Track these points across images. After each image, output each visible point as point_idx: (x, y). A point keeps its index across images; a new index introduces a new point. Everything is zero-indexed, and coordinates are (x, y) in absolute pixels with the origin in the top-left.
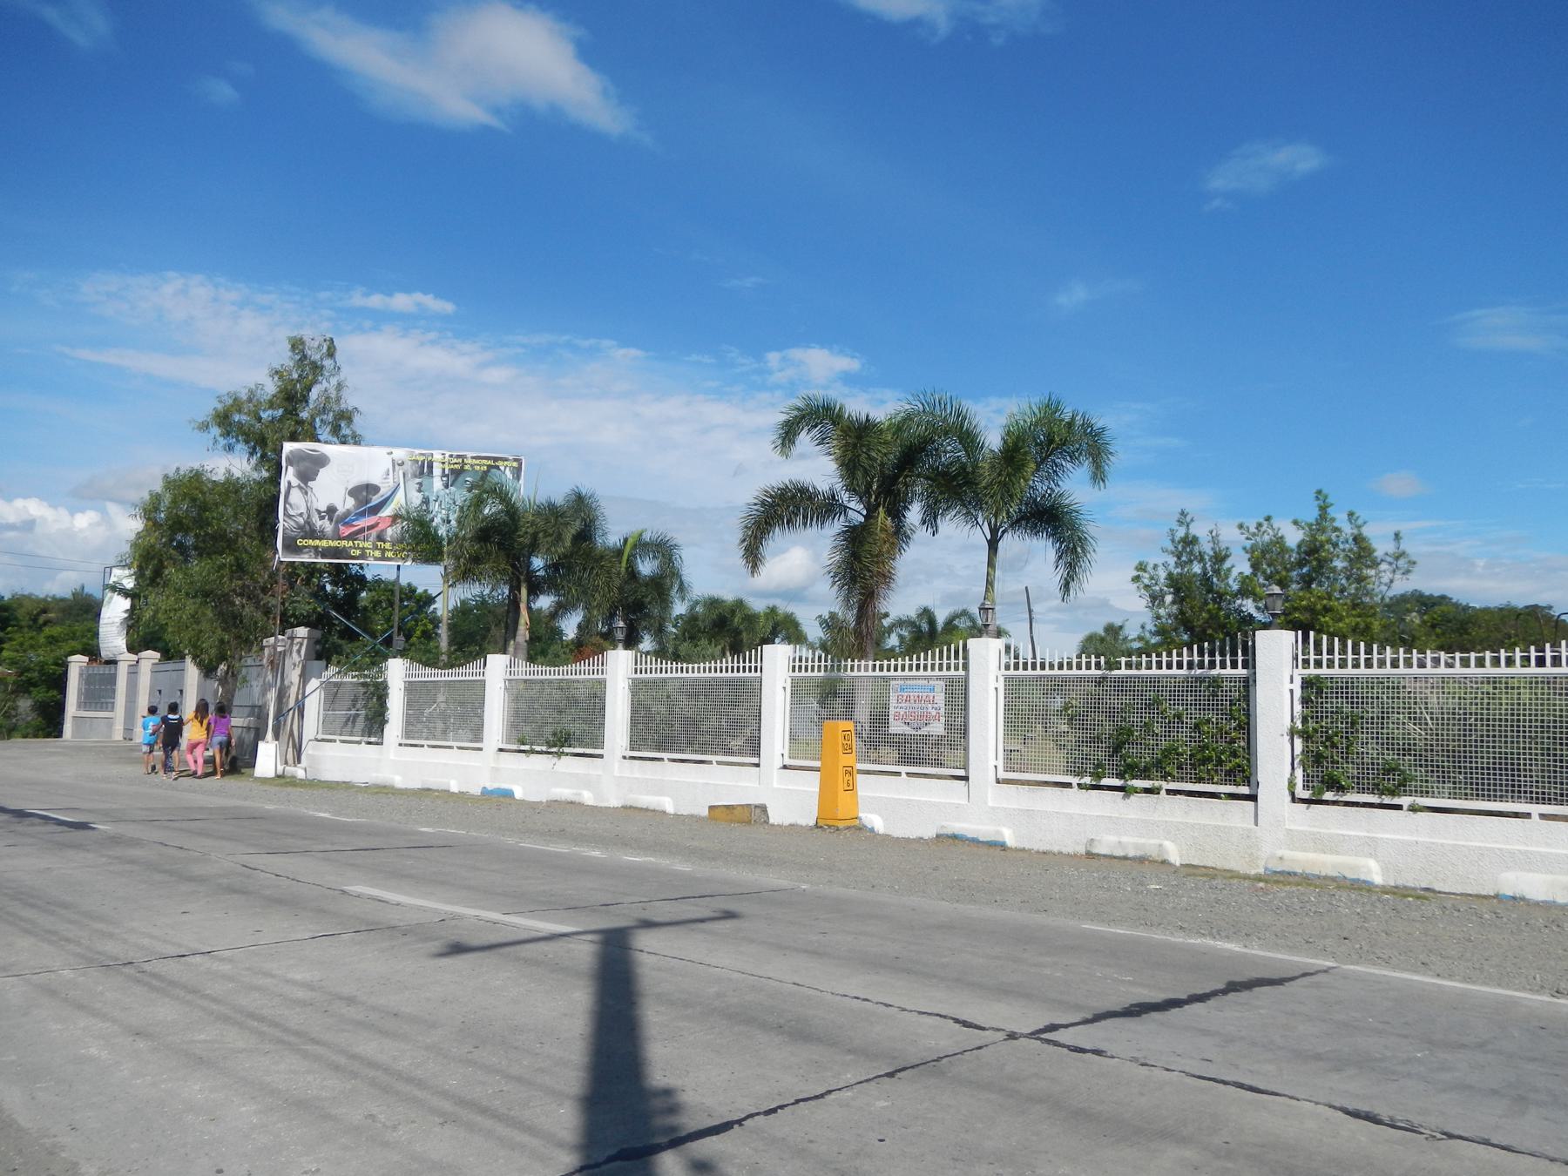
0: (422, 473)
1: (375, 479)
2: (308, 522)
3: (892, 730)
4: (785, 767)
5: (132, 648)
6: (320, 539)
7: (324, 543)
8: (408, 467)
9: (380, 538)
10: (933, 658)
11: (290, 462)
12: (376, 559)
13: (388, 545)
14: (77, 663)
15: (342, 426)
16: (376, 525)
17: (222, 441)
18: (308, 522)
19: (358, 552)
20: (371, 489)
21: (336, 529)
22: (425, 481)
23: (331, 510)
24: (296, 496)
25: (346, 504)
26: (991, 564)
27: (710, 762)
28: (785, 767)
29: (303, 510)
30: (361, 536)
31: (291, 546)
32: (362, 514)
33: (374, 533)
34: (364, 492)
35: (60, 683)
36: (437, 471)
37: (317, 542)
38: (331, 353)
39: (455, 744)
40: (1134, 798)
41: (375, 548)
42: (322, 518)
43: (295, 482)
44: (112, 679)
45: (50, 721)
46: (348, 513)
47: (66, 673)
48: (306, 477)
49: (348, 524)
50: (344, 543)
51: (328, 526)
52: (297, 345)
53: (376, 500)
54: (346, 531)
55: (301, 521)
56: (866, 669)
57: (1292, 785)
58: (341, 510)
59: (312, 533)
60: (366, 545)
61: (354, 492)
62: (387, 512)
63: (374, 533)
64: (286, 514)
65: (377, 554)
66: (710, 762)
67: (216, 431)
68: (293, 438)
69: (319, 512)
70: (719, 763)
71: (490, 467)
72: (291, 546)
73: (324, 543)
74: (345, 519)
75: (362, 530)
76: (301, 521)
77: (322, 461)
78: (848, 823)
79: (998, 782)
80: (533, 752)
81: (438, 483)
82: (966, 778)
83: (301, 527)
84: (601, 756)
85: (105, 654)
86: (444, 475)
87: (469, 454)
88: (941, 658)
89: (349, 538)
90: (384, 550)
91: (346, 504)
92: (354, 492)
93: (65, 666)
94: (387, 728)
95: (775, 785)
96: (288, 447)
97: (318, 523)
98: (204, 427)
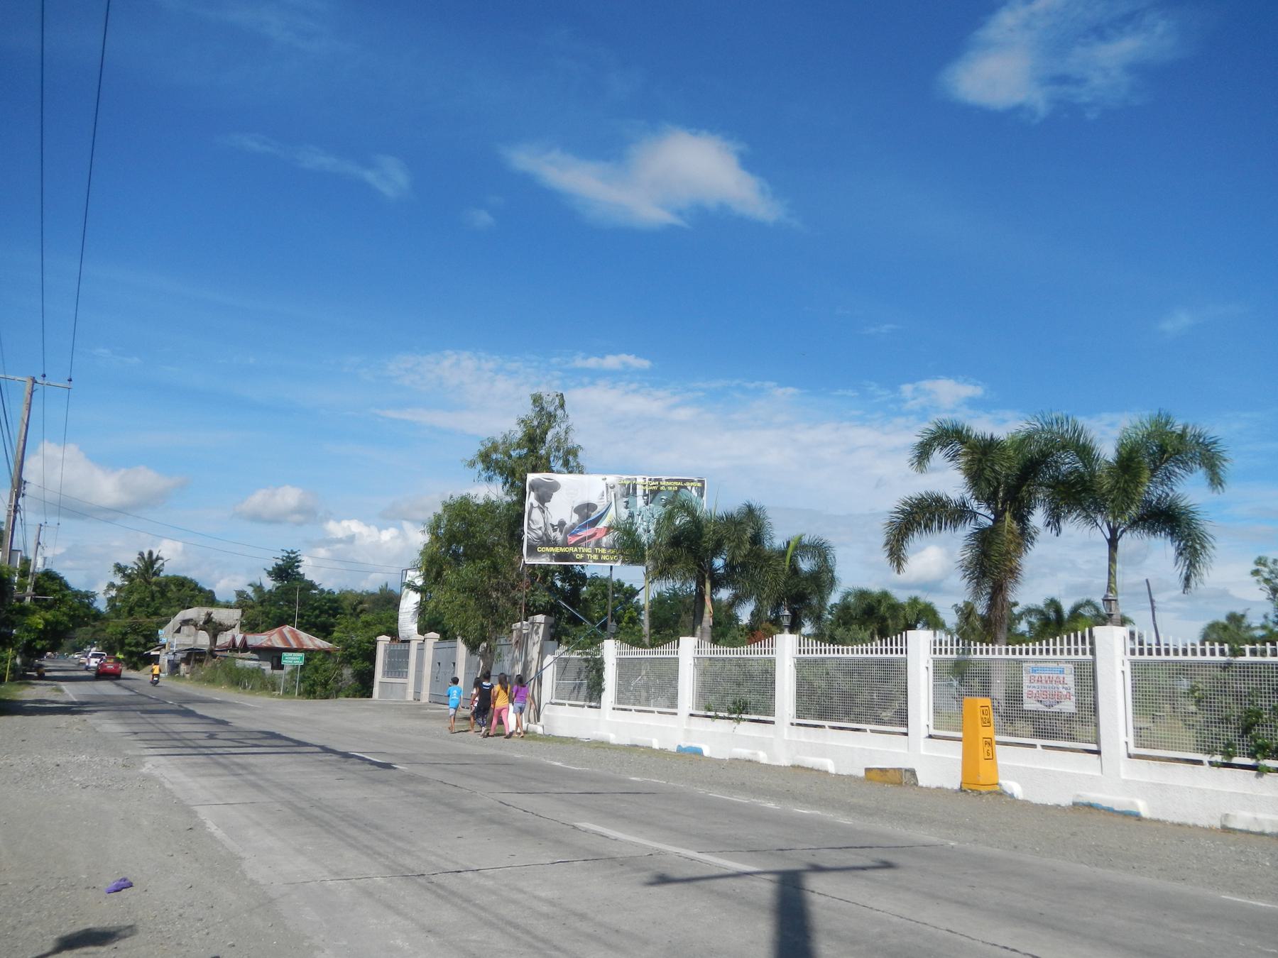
0: (628, 494)
1: (594, 500)
2: (545, 534)
3: (1027, 706)
4: (930, 737)
5: (422, 631)
7: (557, 550)
8: (618, 489)
9: (598, 544)
10: (1062, 644)
11: (532, 488)
12: (595, 561)
13: (603, 551)
14: (383, 641)
15: (570, 461)
16: (594, 535)
17: (484, 475)
18: (545, 534)
20: (590, 507)
21: (565, 538)
22: (631, 499)
23: (562, 524)
24: (536, 514)
25: (572, 519)
26: (1112, 559)
27: (865, 730)
28: (930, 737)
29: (542, 525)
31: (532, 550)
32: (584, 527)
33: (593, 541)
34: (585, 510)
35: (371, 656)
36: (640, 492)
38: (562, 406)
39: (656, 709)
40: (1268, 777)
41: (594, 552)
42: (555, 530)
43: (536, 503)
44: (406, 654)
45: (364, 686)
46: (573, 527)
47: (375, 649)
48: (543, 499)
49: (573, 535)
50: (571, 549)
51: (559, 536)
52: (537, 400)
53: (594, 515)
54: (572, 540)
55: (540, 533)
56: (1000, 653)
58: (569, 523)
61: (578, 510)
62: (603, 524)
63: (593, 541)
65: (595, 557)
66: (865, 730)
67: (480, 466)
68: (534, 470)
70: (872, 731)
71: (679, 487)
73: (557, 550)
74: (572, 531)
75: (584, 539)
76: (540, 533)
77: (554, 487)
79: (1130, 756)
80: (717, 717)
81: (640, 502)
82: (1098, 752)
83: (540, 538)
84: (773, 723)
85: (402, 636)
86: (645, 495)
87: (664, 478)
88: (1069, 644)
89: (573, 545)
90: (600, 555)
91: (572, 519)
92: (578, 510)
93: (375, 643)
94: (604, 695)
95: (923, 752)
96: (531, 477)
98: (472, 464)
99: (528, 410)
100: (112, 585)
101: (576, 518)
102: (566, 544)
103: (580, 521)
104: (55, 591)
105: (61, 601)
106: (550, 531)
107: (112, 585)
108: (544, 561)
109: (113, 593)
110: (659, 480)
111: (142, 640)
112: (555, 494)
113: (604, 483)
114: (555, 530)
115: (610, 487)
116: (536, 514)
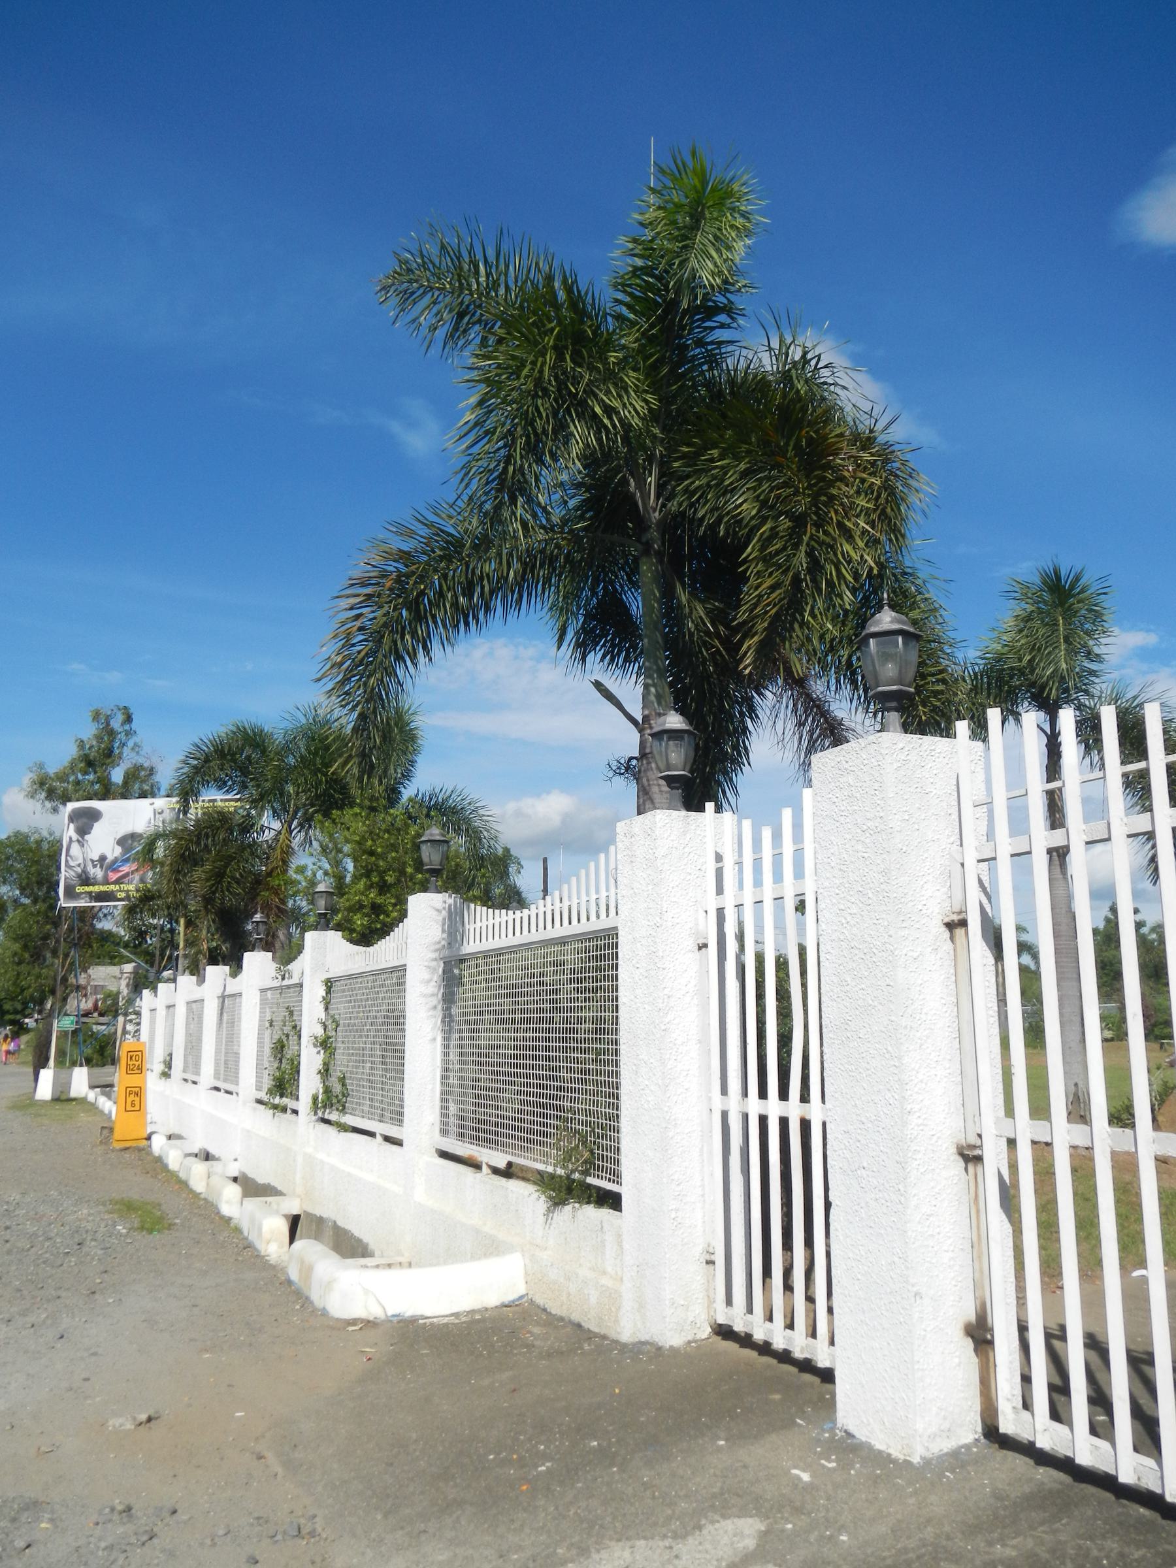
2: (84, 871)
6: (93, 885)
8: (168, 815)
17: (48, 805)
18: (84, 871)
19: (123, 895)
20: (133, 836)
21: (106, 877)
23: (103, 859)
24: (75, 848)
28: (217, 1089)
29: (81, 861)
30: (126, 880)
31: (70, 893)
32: (127, 860)
33: (137, 877)
37: (91, 888)
42: (95, 866)
43: (75, 837)
46: (116, 860)
48: (83, 831)
49: (115, 870)
50: (112, 887)
51: (97, 873)
52: (96, 716)
54: (113, 877)
57: (315, 1099)
58: (110, 858)
59: (85, 880)
61: (121, 842)
64: (67, 865)
69: (93, 861)
72: (70, 893)
74: (113, 866)
75: (127, 875)
76: (79, 870)
77: (95, 816)
78: (128, 1144)
83: (79, 876)
92: (121, 842)
99: (88, 731)
101: (118, 850)
102: (106, 882)
103: (123, 854)
108: (82, 903)
110: (214, 801)
112: (97, 826)
113: (151, 809)
114: (95, 866)
116: (75, 848)
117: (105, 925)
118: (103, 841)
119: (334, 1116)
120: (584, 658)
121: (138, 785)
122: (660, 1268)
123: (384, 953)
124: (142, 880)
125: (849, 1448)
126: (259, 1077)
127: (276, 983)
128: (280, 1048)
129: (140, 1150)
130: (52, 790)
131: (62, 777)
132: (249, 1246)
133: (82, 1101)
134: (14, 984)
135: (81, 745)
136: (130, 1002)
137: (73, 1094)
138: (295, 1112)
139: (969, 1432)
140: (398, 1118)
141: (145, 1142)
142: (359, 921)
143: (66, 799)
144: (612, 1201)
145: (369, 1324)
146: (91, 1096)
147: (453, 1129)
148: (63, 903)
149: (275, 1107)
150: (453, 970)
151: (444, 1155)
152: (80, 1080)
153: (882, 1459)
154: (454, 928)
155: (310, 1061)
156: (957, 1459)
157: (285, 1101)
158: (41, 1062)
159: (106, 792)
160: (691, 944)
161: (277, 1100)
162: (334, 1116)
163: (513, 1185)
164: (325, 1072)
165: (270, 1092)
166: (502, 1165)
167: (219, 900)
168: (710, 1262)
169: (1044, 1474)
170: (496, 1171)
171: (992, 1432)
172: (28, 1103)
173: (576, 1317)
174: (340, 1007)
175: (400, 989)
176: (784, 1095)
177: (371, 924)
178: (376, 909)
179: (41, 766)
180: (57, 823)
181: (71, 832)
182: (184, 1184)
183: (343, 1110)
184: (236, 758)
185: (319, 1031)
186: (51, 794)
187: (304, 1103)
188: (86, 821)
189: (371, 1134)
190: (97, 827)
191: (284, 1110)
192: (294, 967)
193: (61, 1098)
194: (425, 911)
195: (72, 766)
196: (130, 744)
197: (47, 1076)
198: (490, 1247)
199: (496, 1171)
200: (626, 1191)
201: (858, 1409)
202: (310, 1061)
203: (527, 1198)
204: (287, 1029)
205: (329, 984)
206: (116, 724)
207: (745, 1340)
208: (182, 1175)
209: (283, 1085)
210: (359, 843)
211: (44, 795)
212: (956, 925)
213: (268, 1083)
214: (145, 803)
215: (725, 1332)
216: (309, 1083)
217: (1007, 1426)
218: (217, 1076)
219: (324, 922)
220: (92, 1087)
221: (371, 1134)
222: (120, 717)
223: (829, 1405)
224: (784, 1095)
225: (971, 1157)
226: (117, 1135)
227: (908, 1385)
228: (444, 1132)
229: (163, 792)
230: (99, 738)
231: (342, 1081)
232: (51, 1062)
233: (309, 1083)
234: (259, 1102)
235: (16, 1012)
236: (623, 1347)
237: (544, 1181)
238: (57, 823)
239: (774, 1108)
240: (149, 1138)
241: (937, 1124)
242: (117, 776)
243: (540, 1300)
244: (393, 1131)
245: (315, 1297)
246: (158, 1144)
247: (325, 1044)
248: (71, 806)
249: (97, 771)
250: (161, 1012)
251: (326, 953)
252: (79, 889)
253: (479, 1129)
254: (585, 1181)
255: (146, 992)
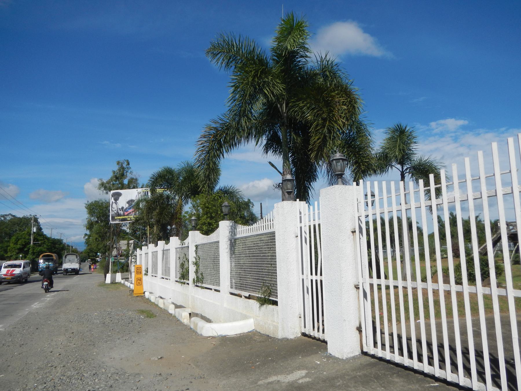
1: (134, 198)
2: (117, 212)
8: (142, 194)
17: (105, 192)
18: (117, 212)
20: (132, 201)
21: (124, 213)
23: (123, 208)
24: (114, 205)
25: (126, 206)
28: (163, 278)
32: (130, 208)
34: (130, 202)
37: (120, 217)
38: (129, 164)
43: (114, 201)
46: (126, 208)
48: (116, 200)
51: (121, 212)
52: (118, 163)
54: (126, 213)
57: (194, 280)
58: (125, 208)
59: (119, 215)
60: (132, 217)
61: (128, 202)
64: (112, 210)
74: (126, 210)
76: (116, 212)
77: (119, 195)
83: (116, 214)
89: (127, 215)
91: (126, 206)
92: (128, 202)
97: (120, 212)
99: (116, 168)
100: (86, 235)
101: (127, 205)
102: (124, 215)
104: (41, 240)
105: (44, 243)
106: (119, 211)
107: (86, 235)
108: (117, 222)
109: (87, 237)
111: (94, 254)
115: (139, 193)
116: (114, 205)
117: (124, 228)
118: (122, 202)
119: (200, 285)
120: (267, 152)
121: (133, 184)
122: (287, 320)
123: (213, 237)
124: (135, 215)
125: (330, 357)
126: (176, 274)
127: (180, 246)
128: (182, 265)
129: (142, 296)
130: (106, 187)
131: (108, 183)
132: (178, 320)
133: (120, 283)
134: (97, 248)
135: (114, 172)
136: (133, 252)
137: (117, 281)
138: (188, 284)
139: (358, 352)
140: (218, 284)
141: (143, 294)
142: (205, 228)
143: (110, 190)
144: (275, 303)
145: (213, 337)
146: (123, 282)
147: (234, 287)
148: (111, 222)
149: (182, 283)
150: (233, 243)
151: (232, 294)
152: (119, 277)
153: (337, 359)
154: (233, 231)
155: (192, 269)
156: (354, 358)
157: (185, 281)
158: (107, 272)
159: (123, 187)
160: (294, 236)
161: (182, 281)
162: (200, 285)
163: (251, 301)
164: (197, 272)
165: (180, 278)
166: (247, 295)
167: (160, 220)
168: (300, 317)
169: (373, 360)
170: (246, 297)
171: (362, 351)
172: (103, 284)
173: (267, 334)
174: (200, 253)
175: (218, 247)
176: (316, 274)
177: (209, 229)
178: (210, 224)
179: (101, 180)
180: (109, 197)
181: (112, 200)
182: (157, 305)
183: (202, 283)
184: (165, 178)
185: (194, 260)
186: (105, 188)
187: (191, 281)
188: (117, 196)
189: (211, 289)
190: (121, 198)
191: (184, 283)
192: (186, 241)
193: (113, 282)
194: (224, 225)
195: (111, 179)
196: (129, 171)
197: (109, 276)
198: (245, 317)
199: (246, 297)
200: (279, 300)
201: (333, 349)
202: (192, 269)
203: (254, 304)
204: (184, 260)
205: (197, 246)
206: (125, 165)
207: (310, 336)
208: (156, 303)
209: (184, 276)
210: (204, 205)
211: (103, 188)
212: (354, 232)
213: (179, 275)
214: (135, 190)
215: (304, 334)
216: (192, 275)
217: (365, 350)
218: (163, 274)
219: (195, 228)
220: (122, 279)
221: (211, 289)
222: (126, 163)
223: (326, 349)
224: (316, 274)
225: (357, 288)
226: (135, 292)
227: (343, 343)
228: (232, 288)
229: (140, 186)
230: (119, 170)
231: (202, 274)
232: (110, 272)
233: (192, 275)
234: (176, 281)
235: (93, 256)
236: (279, 340)
237: (259, 299)
238: (109, 197)
239: (314, 277)
240: (144, 293)
241: (350, 280)
242: (126, 182)
243: (258, 330)
244: (217, 288)
245: (199, 331)
246: (147, 295)
247: (196, 264)
248: (112, 192)
249: (120, 180)
250: (144, 255)
251: (195, 237)
252: (116, 218)
253: (241, 286)
254: (269, 299)
255: (138, 249)
